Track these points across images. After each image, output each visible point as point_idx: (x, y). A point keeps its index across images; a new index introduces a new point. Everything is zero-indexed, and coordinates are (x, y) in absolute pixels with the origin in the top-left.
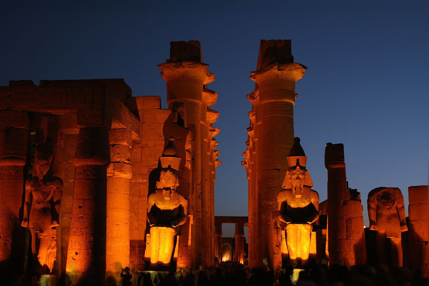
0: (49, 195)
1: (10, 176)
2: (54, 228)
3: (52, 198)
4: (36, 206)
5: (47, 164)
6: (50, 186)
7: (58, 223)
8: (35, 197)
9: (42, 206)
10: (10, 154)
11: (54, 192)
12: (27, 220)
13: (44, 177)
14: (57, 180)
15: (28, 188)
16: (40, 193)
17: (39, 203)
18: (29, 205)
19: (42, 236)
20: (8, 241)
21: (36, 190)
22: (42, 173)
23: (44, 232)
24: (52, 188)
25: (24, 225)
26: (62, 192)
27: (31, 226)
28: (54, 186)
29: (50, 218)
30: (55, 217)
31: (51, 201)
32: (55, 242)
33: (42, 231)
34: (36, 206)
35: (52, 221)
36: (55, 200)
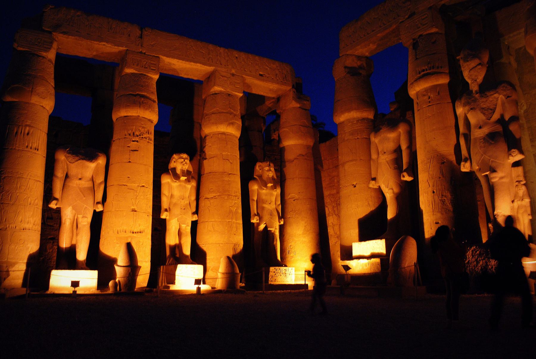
0: (494, 112)
1: (430, 102)
2: (516, 164)
3: (502, 116)
4: (478, 134)
5: (480, 64)
6: (493, 96)
7: (521, 152)
8: (473, 121)
9: (486, 130)
10: (423, 71)
11: (503, 104)
12: (469, 159)
13: (481, 86)
14: (503, 85)
15: (460, 111)
16: (479, 112)
17: (480, 128)
18: (467, 137)
19: (495, 178)
20: (445, 197)
21: (472, 109)
22: (476, 81)
23: (499, 171)
24: (497, 99)
25: (465, 168)
26: (517, 103)
27: (476, 168)
28: (500, 94)
29: (504, 146)
30: (514, 144)
31: (501, 121)
32: (524, 188)
33: (493, 171)
34: (478, 134)
35: (509, 149)
36: (507, 118)
